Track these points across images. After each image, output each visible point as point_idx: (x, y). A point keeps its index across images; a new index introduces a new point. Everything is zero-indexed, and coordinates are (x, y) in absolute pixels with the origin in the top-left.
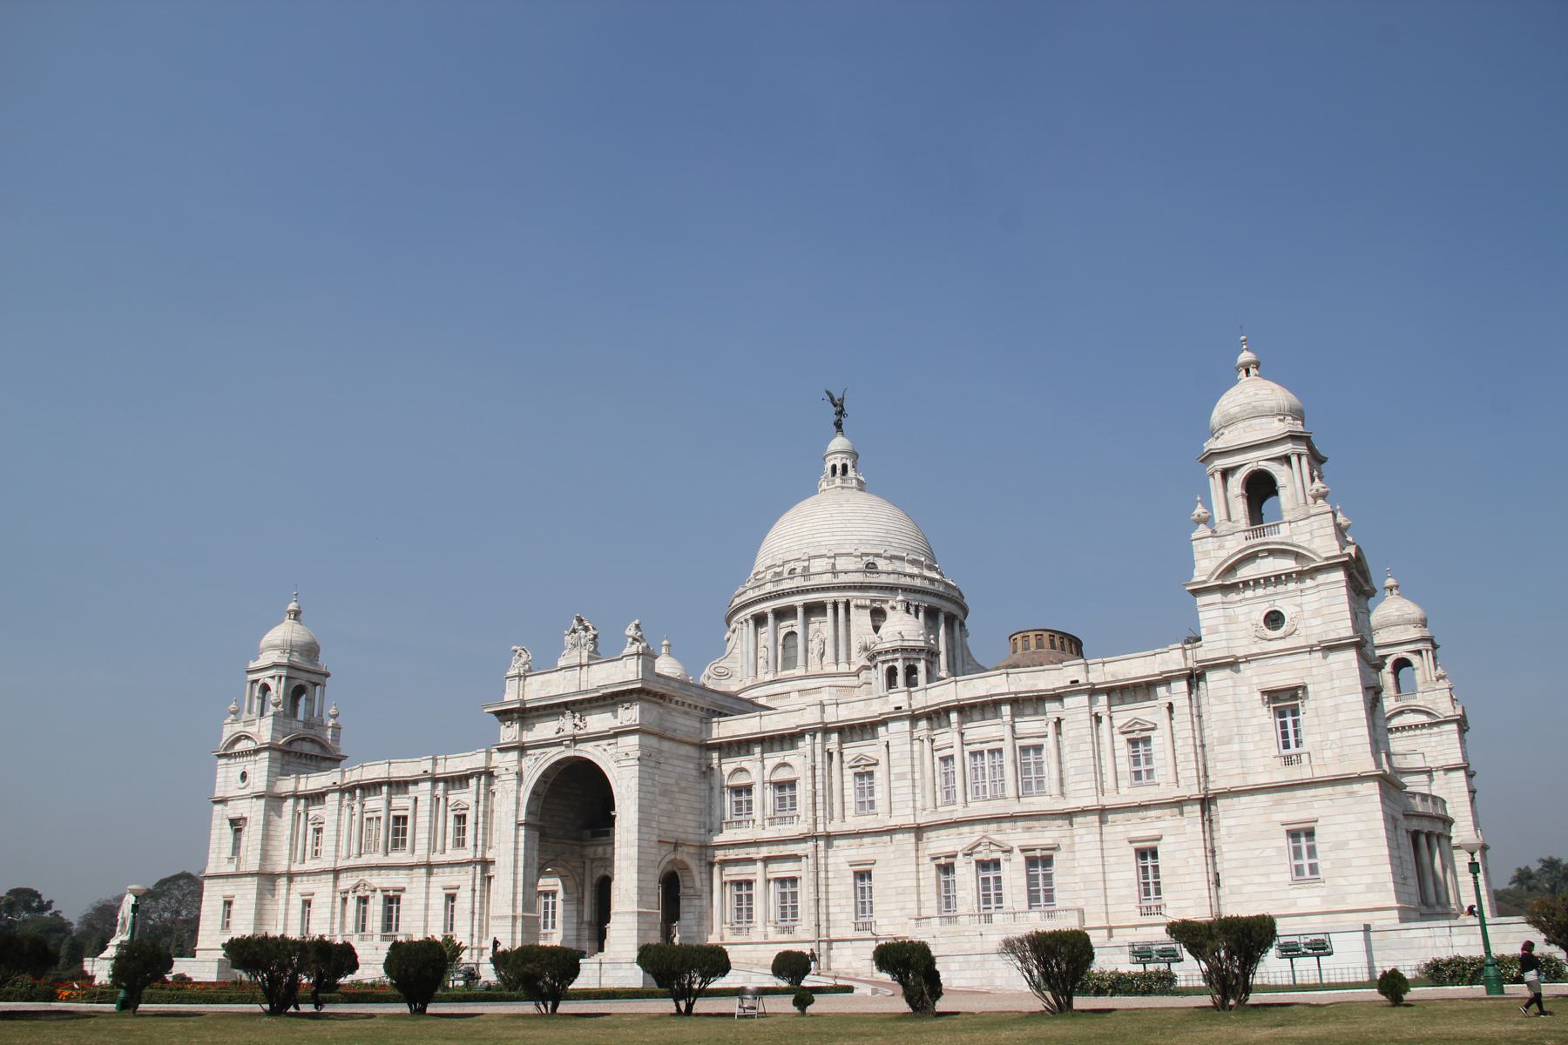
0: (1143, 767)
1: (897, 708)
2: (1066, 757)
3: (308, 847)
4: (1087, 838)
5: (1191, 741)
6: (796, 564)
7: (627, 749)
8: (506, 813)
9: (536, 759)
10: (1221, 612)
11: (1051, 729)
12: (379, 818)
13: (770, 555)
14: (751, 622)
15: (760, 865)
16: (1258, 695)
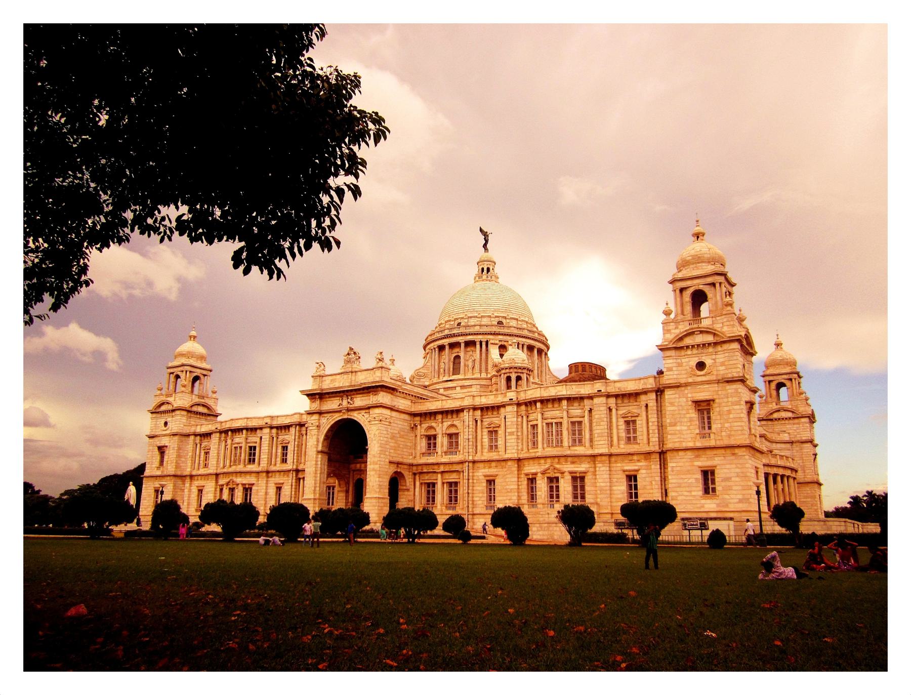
0: (632, 435)
1: (510, 399)
2: (594, 428)
3: (201, 462)
5: (656, 423)
7: (375, 416)
10: (675, 361)
11: (587, 414)
14: (437, 349)
15: (439, 476)
16: (690, 403)
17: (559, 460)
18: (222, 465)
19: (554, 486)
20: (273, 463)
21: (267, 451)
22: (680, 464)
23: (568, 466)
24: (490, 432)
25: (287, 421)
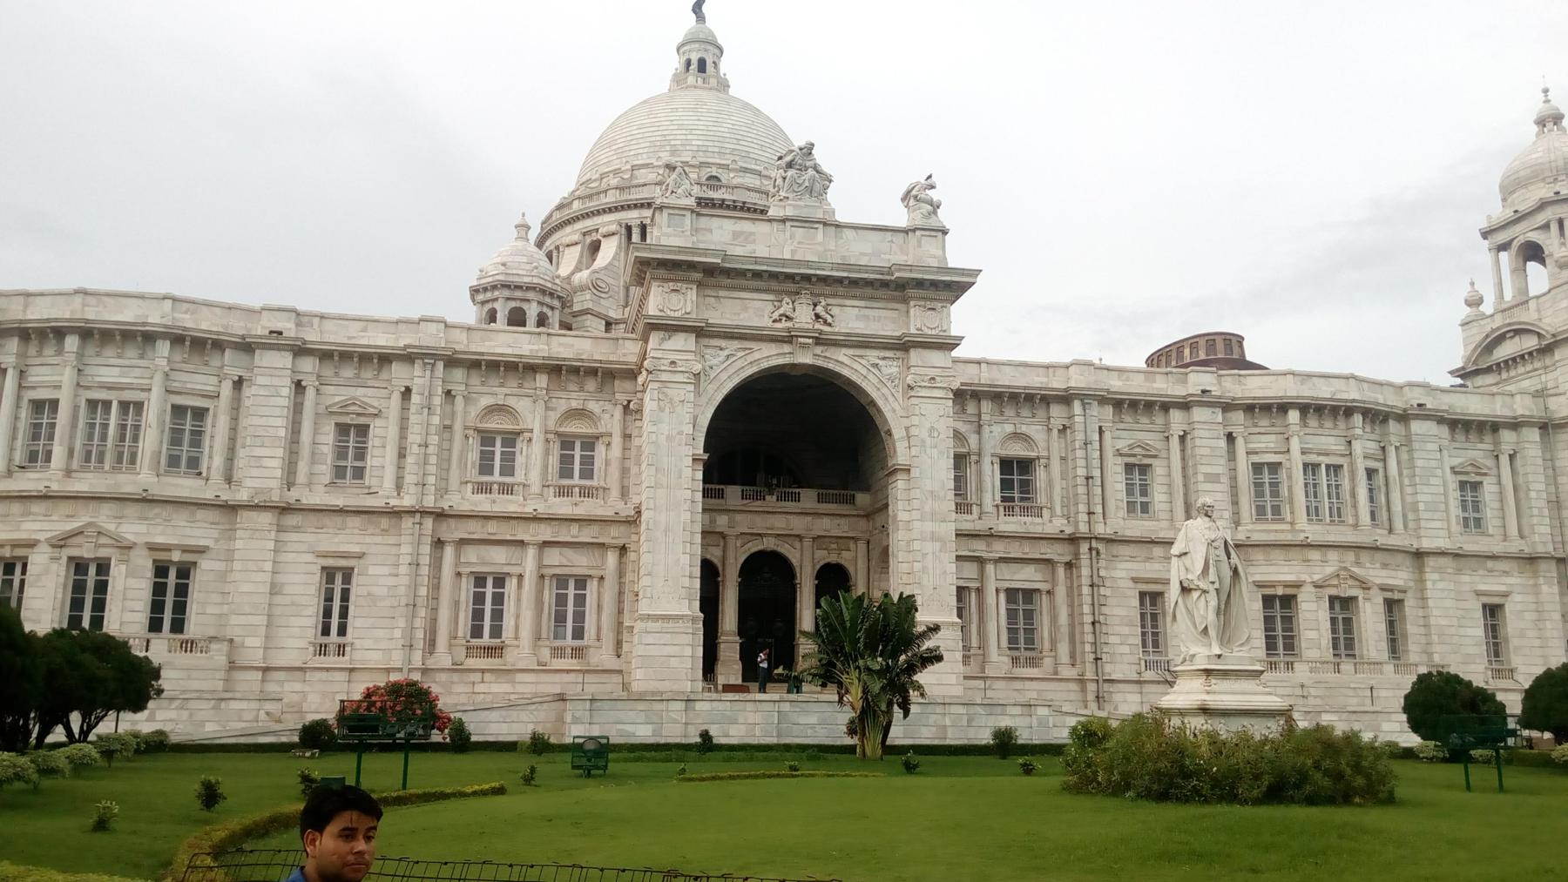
1: (1204, 392)
4: (1441, 585)
5: (1544, 495)
6: (720, 171)
7: (932, 372)
8: (668, 437)
9: (728, 357)
12: (131, 408)
13: (668, 148)
17: (1357, 556)
19: (1340, 617)
20: (301, 477)
21: (282, 433)
24: (1129, 468)
25: (381, 340)
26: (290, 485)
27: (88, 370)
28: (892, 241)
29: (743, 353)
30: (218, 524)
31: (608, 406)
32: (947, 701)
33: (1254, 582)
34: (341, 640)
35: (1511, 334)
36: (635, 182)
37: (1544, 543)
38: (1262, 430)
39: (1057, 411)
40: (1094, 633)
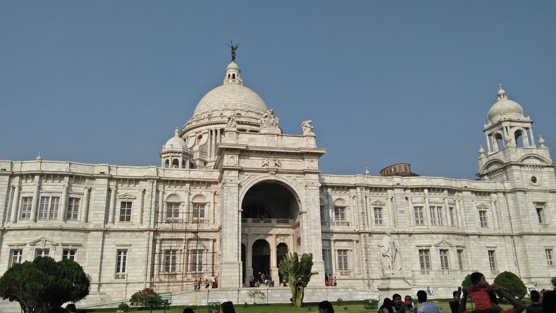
1: (398, 184)
4: (475, 245)
8: (230, 204)
9: (248, 178)
10: (520, 173)
13: (224, 104)
16: (531, 203)
17: (448, 236)
18: (12, 218)
20: (110, 219)
21: (105, 205)
22: (533, 244)
23: (454, 241)
24: (375, 209)
26: (106, 222)
27: (42, 187)
28: (299, 140)
29: (252, 177)
30: (83, 236)
31: (209, 193)
32: (321, 288)
33: (416, 245)
34: (123, 273)
35: (492, 163)
36: (213, 116)
37: (506, 230)
38: (417, 196)
39: (352, 191)
40: (366, 263)
